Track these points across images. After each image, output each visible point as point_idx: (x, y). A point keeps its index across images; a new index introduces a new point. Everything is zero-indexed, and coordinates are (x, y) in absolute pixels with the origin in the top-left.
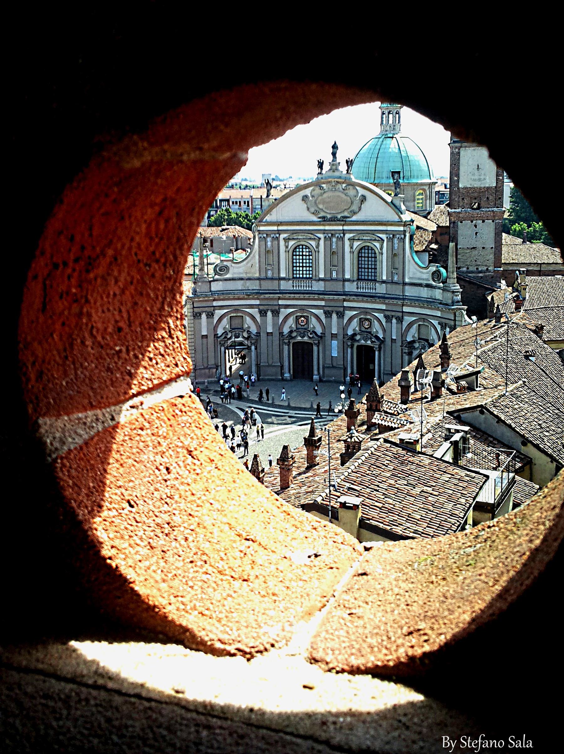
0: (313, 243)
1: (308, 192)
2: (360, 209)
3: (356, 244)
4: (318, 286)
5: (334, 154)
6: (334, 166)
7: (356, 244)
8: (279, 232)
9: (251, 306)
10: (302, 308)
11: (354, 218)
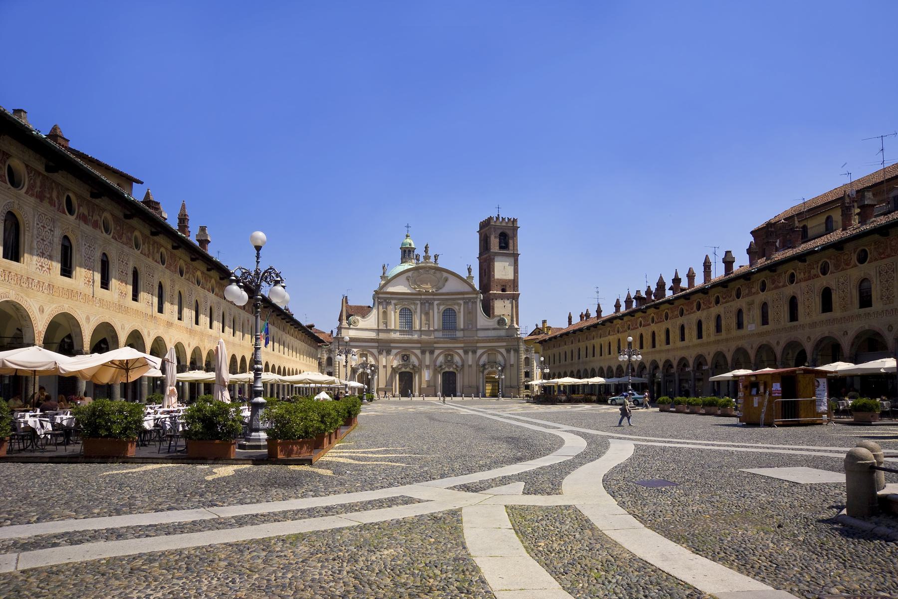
0: (413, 307)
1: (410, 274)
3: (442, 307)
4: (416, 337)
5: (426, 251)
6: (427, 258)
7: (442, 307)
9: (373, 347)
10: (405, 349)
11: (440, 291)
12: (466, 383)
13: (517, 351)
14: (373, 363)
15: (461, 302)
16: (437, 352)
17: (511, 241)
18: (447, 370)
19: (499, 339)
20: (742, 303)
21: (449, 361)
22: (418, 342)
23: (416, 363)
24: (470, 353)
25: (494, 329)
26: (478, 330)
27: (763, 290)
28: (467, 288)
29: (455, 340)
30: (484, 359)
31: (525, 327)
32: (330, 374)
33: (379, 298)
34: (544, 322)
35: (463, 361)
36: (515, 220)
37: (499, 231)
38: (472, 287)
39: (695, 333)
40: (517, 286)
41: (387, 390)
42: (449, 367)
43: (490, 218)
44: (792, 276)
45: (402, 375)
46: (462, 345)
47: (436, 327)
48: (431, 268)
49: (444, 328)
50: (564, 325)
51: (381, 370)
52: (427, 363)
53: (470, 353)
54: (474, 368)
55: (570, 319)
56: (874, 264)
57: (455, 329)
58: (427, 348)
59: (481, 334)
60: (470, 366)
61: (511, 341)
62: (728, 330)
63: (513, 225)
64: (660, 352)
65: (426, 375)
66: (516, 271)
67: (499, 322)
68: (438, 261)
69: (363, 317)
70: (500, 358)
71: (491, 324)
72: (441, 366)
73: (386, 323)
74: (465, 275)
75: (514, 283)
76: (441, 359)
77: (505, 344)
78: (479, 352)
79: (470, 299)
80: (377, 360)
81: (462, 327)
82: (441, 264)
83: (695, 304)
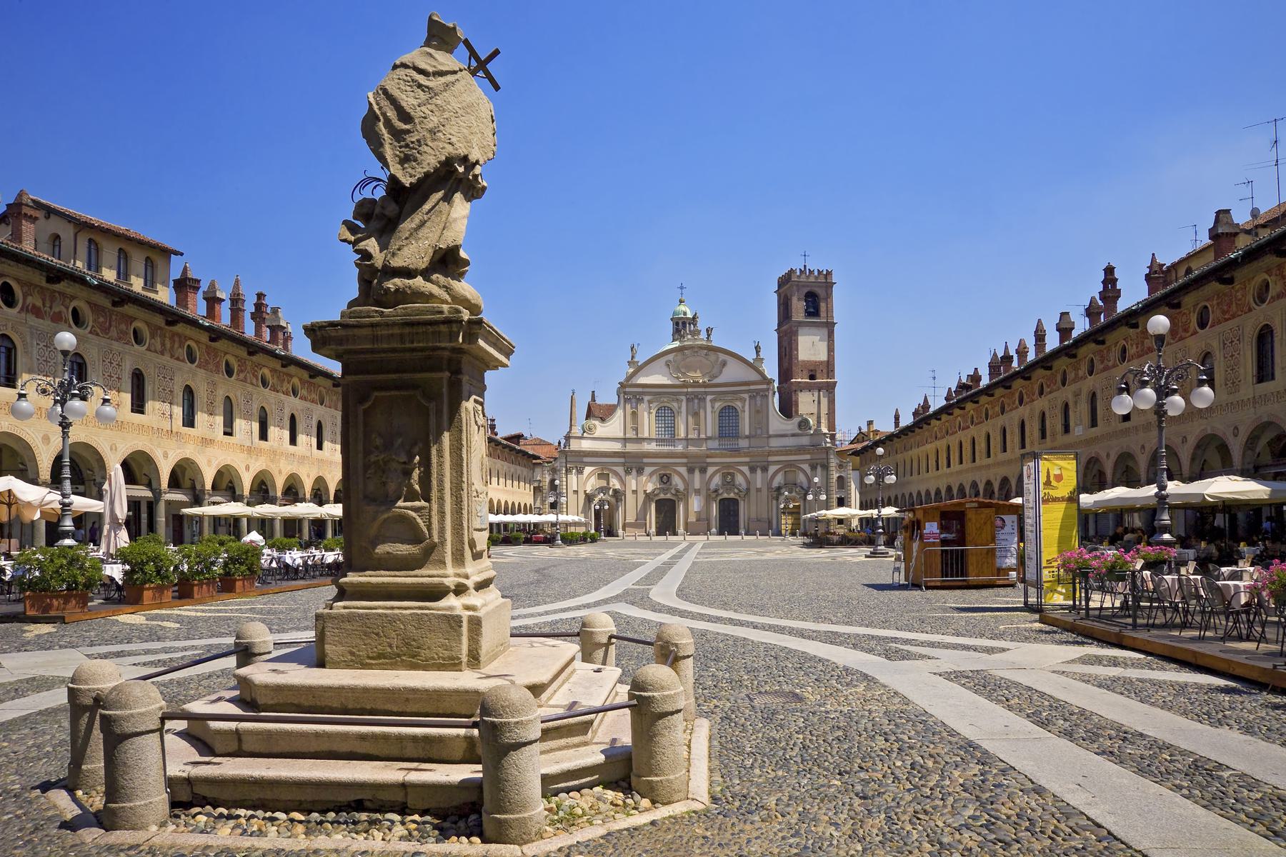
0: (675, 404)
1: (670, 357)
2: (721, 372)
4: (680, 448)
7: (718, 405)
8: (644, 393)
9: (616, 464)
10: (665, 466)
12: (753, 515)
13: (826, 467)
14: (618, 486)
15: (746, 396)
16: (711, 470)
17: (823, 306)
18: (725, 496)
19: (800, 450)
20: (1066, 393)
21: (729, 483)
22: (682, 455)
23: (681, 487)
24: (759, 472)
25: (793, 435)
26: (770, 437)
27: (1091, 373)
28: (754, 376)
29: (736, 451)
30: (779, 480)
31: (846, 431)
32: (554, 506)
33: (625, 393)
34: (870, 423)
35: (748, 482)
36: (829, 273)
37: (806, 290)
38: (762, 374)
39: (1017, 439)
40: (833, 371)
41: (640, 523)
42: (728, 491)
43: (792, 271)
44: (1124, 350)
45: (660, 504)
46: (747, 459)
47: (709, 434)
48: (701, 347)
49: (722, 436)
50: (890, 428)
51: (629, 496)
52: (697, 486)
53: (759, 472)
54: (765, 491)
55: (897, 418)
56: (1218, 328)
57: (737, 436)
58: (697, 465)
59: (775, 443)
60: (759, 490)
61: (818, 452)
62: (1053, 435)
63: (826, 281)
64: (980, 468)
65: (696, 504)
66: (831, 350)
67: (800, 426)
68: (712, 338)
69: (603, 420)
70: (801, 478)
71: (790, 427)
72: (716, 491)
73: (636, 430)
74: (750, 356)
75: (829, 367)
76: (717, 480)
77: (808, 457)
78: (772, 469)
79: (758, 392)
80: (623, 483)
81: (747, 433)
82: (716, 342)
83: (1017, 395)
